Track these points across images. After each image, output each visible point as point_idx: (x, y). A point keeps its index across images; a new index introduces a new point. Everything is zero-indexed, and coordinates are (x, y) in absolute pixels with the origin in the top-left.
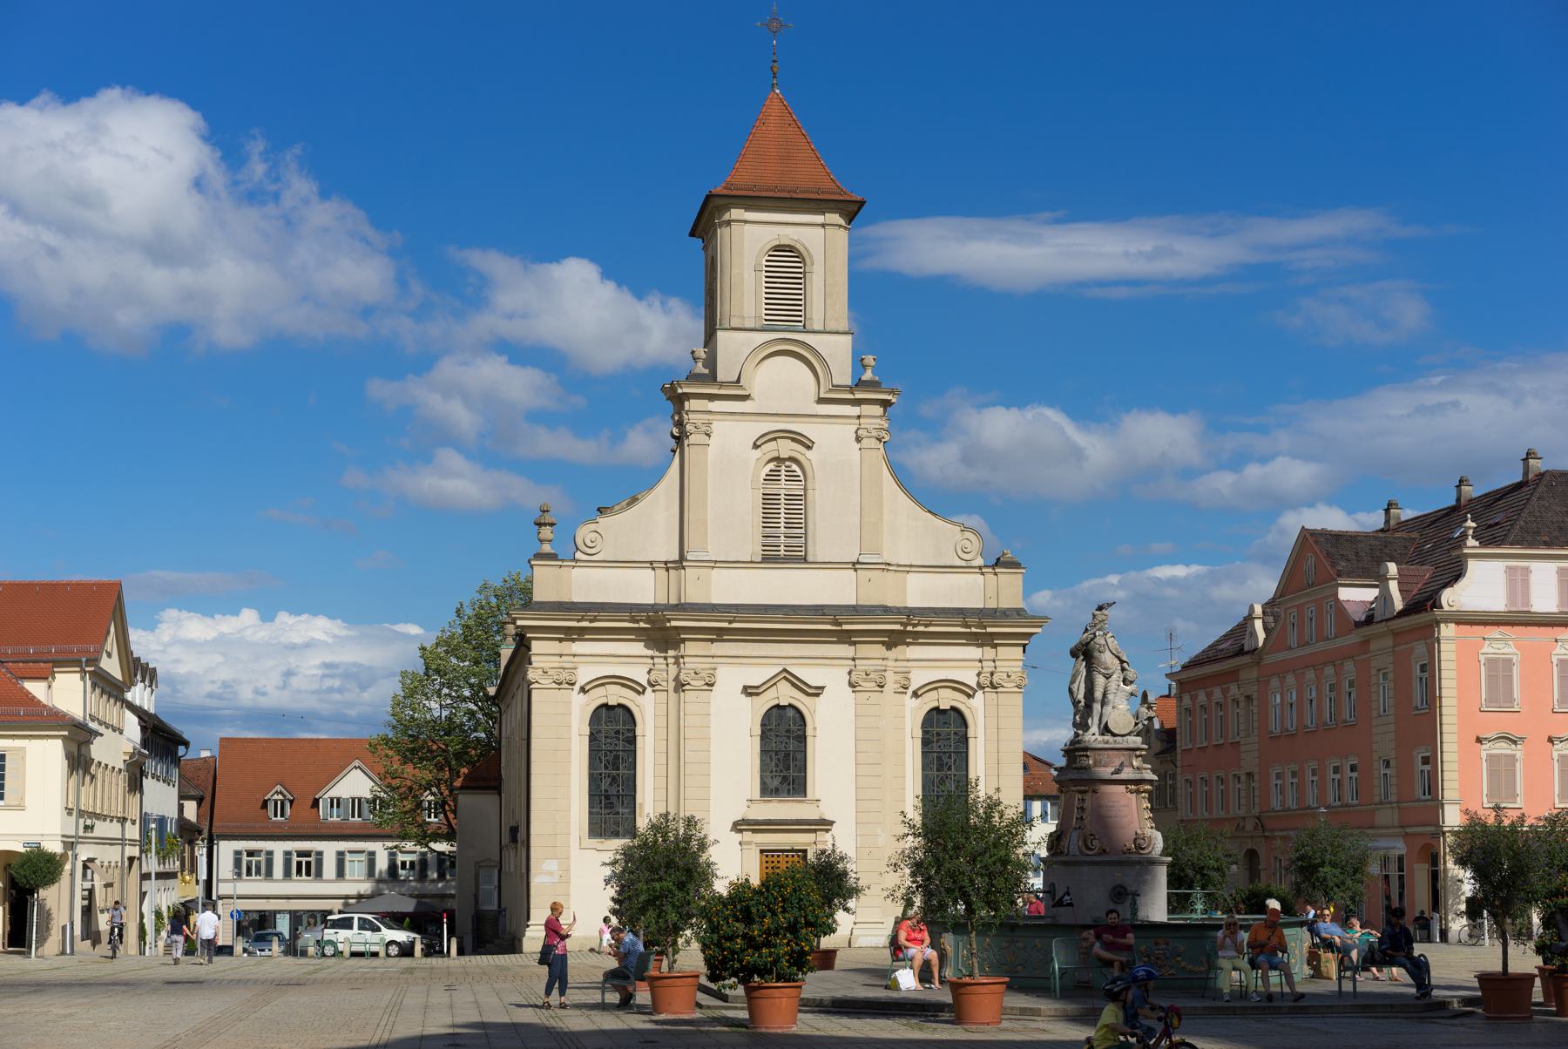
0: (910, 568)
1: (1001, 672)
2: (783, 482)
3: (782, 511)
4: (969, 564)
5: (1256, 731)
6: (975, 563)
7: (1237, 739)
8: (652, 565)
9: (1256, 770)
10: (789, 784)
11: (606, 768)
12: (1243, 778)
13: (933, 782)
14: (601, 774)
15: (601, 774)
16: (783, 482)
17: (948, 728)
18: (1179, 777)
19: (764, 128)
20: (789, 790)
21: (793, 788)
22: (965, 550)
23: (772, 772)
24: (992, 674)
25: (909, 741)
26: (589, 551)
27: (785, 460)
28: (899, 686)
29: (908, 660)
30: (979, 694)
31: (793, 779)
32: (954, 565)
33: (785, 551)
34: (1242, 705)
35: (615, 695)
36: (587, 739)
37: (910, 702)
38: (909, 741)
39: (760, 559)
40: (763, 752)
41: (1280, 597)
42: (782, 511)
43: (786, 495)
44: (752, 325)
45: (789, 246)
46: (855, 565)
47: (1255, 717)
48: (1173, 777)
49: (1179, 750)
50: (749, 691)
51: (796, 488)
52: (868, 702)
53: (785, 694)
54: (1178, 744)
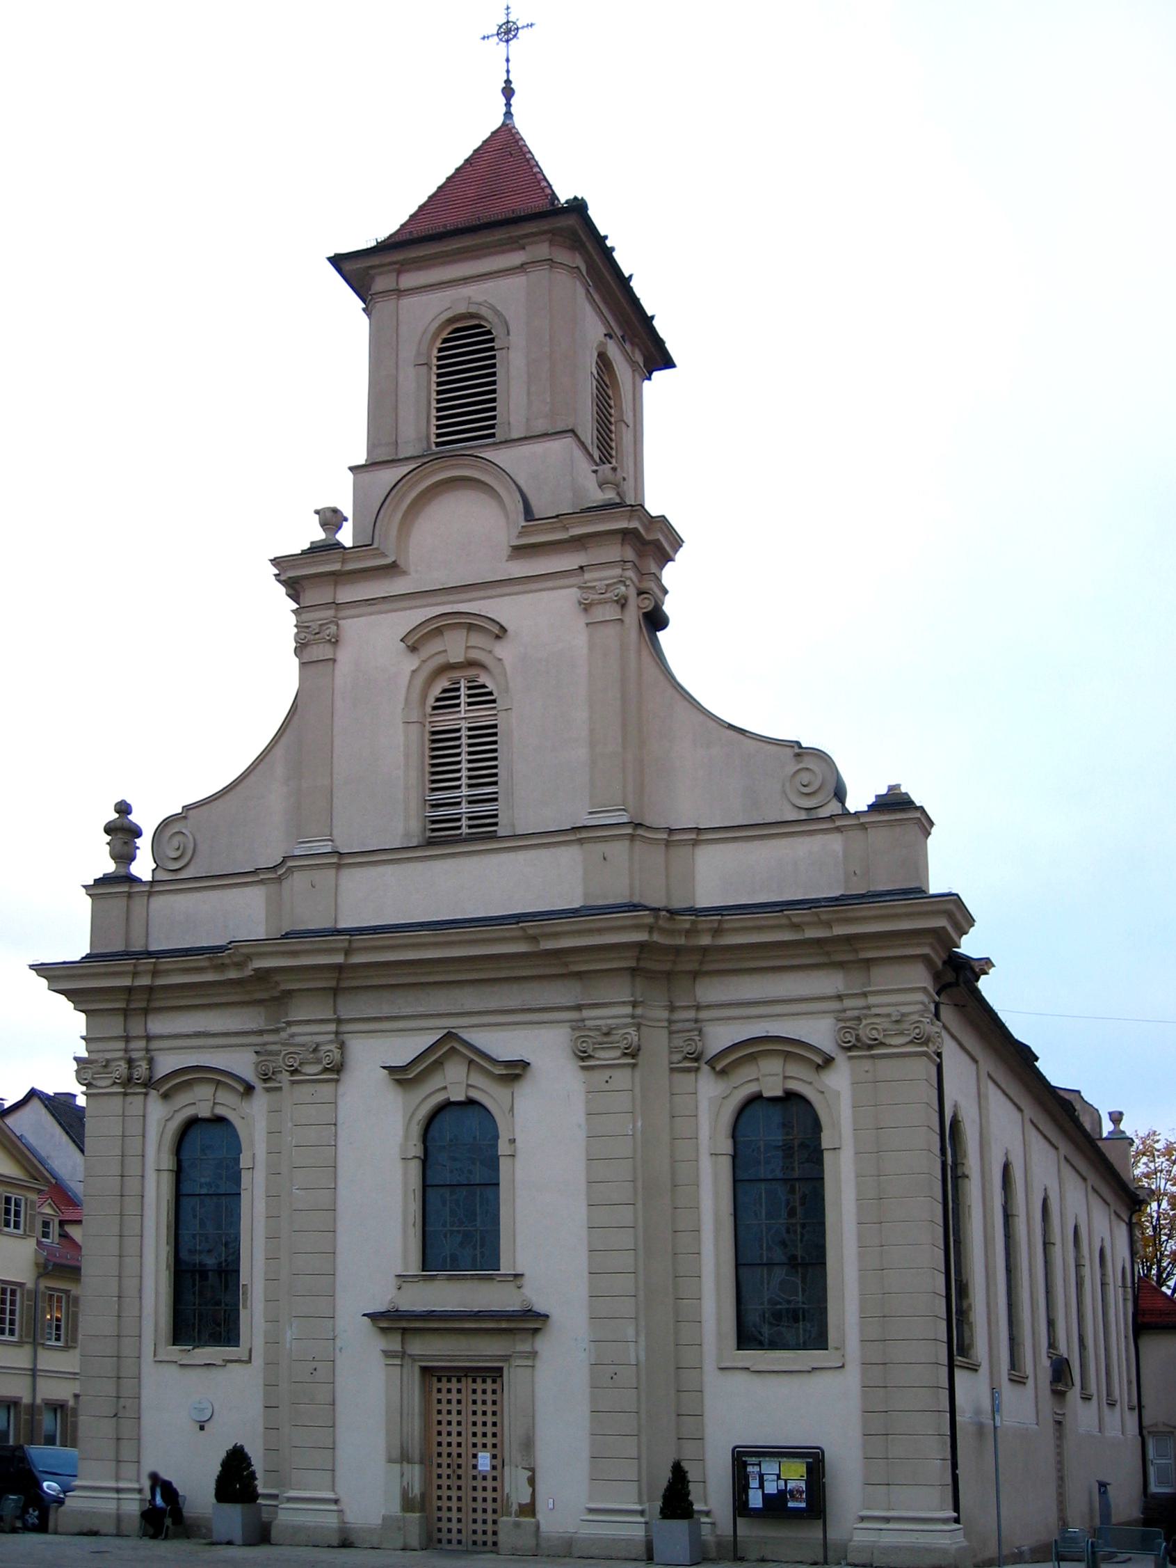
0: (699, 835)
2: (463, 707)
4: (814, 815)
6: (824, 813)
8: (254, 876)
10: (475, 1248)
20: (474, 1259)
21: (481, 1253)
28: (677, 1057)
33: (470, 827)
35: (200, 1101)
37: (708, 1089)
38: (706, 1164)
42: (464, 757)
46: (578, 834)
50: (403, 1077)
51: (482, 715)
52: (607, 1087)
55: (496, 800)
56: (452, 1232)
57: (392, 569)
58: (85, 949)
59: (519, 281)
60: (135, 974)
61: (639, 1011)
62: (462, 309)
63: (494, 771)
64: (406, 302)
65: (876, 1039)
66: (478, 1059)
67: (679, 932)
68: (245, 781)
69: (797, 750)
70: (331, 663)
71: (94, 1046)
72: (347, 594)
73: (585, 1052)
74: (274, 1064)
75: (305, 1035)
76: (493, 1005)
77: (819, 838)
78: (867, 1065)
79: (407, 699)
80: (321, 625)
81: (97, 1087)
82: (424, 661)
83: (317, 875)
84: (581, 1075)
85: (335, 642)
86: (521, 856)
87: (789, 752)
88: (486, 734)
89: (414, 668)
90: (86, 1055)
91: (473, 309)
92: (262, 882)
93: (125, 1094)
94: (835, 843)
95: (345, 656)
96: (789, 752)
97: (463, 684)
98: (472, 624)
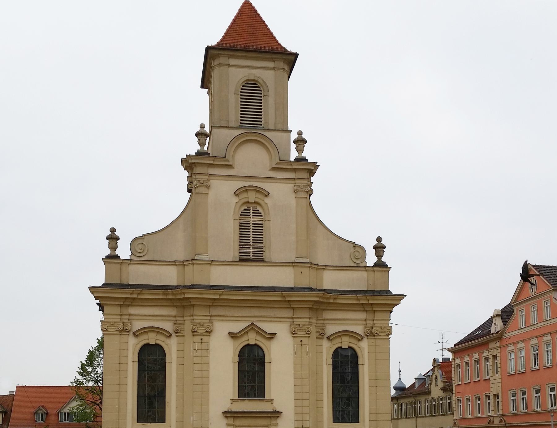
0: (326, 267)
1: (377, 327)
2: (251, 216)
3: (251, 233)
5: (499, 373)
7: (488, 377)
8: (174, 263)
9: (500, 392)
10: (255, 391)
11: (148, 381)
12: (492, 397)
13: (339, 390)
14: (145, 385)
15: (145, 385)
16: (251, 216)
17: (347, 359)
18: (454, 399)
19: (240, 18)
20: (255, 394)
21: (257, 392)
22: (356, 257)
23: (245, 383)
24: (372, 328)
25: (325, 366)
26: (138, 255)
27: (251, 203)
28: (318, 334)
29: (324, 320)
30: (365, 339)
31: (258, 388)
32: (350, 265)
33: (253, 256)
34: (490, 360)
35: (152, 339)
36: (136, 365)
38: (325, 366)
39: (238, 260)
40: (241, 372)
41: (514, 303)
42: (251, 233)
43: (253, 224)
44: (233, 126)
45: (254, 80)
46: (293, 264)
47: (499, 366)
48: (450, 398)
49: (454, 385)
50: (233, 336)
53: (252, 339)
54: (453, 382)
55: (262, 248)
56: (247, 386)
57: (230, 166)
58: (103, 282)
59: (272, 73)
60: (131, 294)
61: (311, 320)
62: (252, 77)
63: (262, 239)
64: (231, 69)
65: (377, 334)
66: (260, 332)
67: (325, 298)
68: (168, 228)
69: (355, 245)
70: (207, 194)
71: (106, 317)
72: (212, 171)
73: (295, 332)
74: (181, 328)
75: (198, 319)
76: (272, 315)
77: (360, 273)
78: (373, 341)
79: (234, 212)
80: (204, 181)
81: (109, 331)
82: (240, 200)
83: (204, 267)
84: (292, 338)
85: (208, 187)
86: (273, 268)
87: (352, 245)
88: (259, 226)
89: (237, 201)
90: (103, 319)
91: (256, 79)
92: (176, 265)
93: (120, 335)
94: (365, 274)
95: (212, 193)
96: (352, 245)
97: (251, 208)
98: (258, 190)
